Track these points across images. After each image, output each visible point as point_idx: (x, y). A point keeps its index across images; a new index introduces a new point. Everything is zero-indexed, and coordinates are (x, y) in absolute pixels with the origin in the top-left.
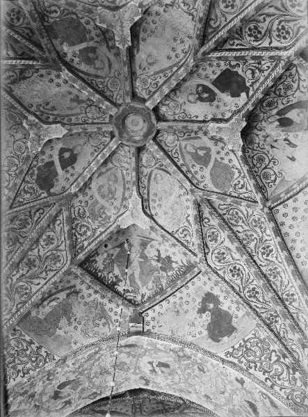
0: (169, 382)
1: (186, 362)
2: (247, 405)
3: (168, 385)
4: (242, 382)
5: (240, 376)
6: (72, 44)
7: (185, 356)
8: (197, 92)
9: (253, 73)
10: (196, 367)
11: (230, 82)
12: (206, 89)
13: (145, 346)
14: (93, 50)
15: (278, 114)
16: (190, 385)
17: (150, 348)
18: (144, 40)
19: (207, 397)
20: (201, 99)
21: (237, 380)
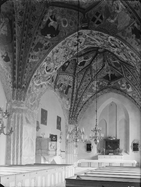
0: (71, 41)
1: (70, 52)
2: (50, 68)
3: (71, 40)
4: (56, 69)
5: (58, 69)
6: (117, 63)
7: (71, 53)
8: (88, 58)
9: (79, 68)
10: (67, 55)
11: (83, 64)
12: (87, 59)
13: (85, 45)
14: (113, 60)
15: (70, 62)
16: (64, 47)
17: (83, 46)
18: (102, 61)
19: (57, 51)
20: (87, 57)
21: (57, 68)
